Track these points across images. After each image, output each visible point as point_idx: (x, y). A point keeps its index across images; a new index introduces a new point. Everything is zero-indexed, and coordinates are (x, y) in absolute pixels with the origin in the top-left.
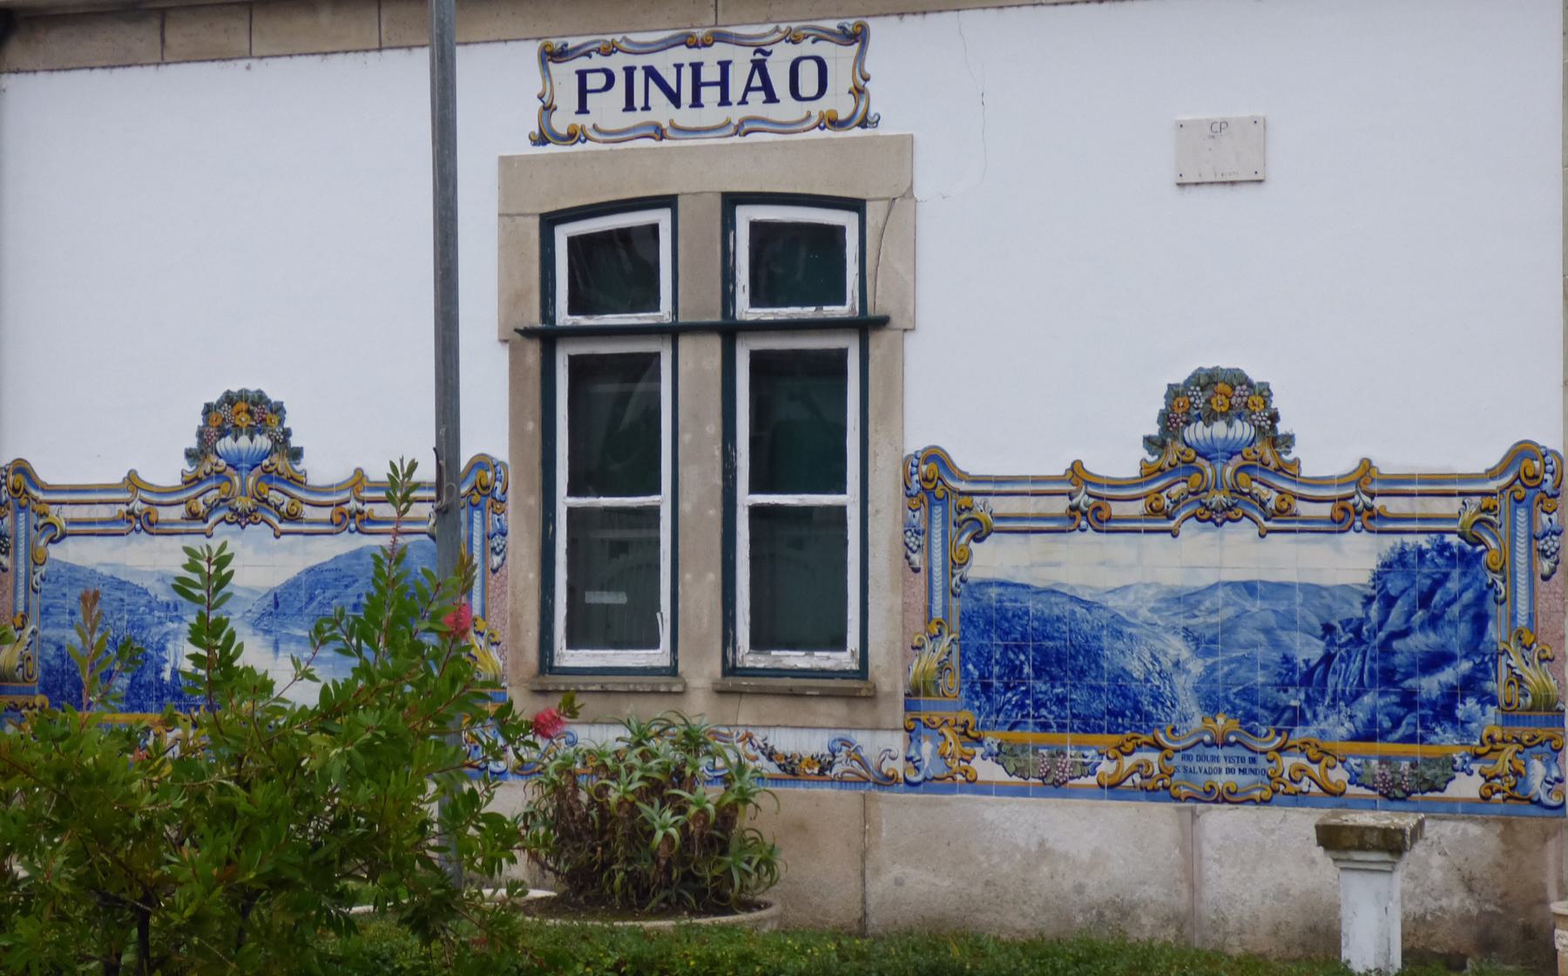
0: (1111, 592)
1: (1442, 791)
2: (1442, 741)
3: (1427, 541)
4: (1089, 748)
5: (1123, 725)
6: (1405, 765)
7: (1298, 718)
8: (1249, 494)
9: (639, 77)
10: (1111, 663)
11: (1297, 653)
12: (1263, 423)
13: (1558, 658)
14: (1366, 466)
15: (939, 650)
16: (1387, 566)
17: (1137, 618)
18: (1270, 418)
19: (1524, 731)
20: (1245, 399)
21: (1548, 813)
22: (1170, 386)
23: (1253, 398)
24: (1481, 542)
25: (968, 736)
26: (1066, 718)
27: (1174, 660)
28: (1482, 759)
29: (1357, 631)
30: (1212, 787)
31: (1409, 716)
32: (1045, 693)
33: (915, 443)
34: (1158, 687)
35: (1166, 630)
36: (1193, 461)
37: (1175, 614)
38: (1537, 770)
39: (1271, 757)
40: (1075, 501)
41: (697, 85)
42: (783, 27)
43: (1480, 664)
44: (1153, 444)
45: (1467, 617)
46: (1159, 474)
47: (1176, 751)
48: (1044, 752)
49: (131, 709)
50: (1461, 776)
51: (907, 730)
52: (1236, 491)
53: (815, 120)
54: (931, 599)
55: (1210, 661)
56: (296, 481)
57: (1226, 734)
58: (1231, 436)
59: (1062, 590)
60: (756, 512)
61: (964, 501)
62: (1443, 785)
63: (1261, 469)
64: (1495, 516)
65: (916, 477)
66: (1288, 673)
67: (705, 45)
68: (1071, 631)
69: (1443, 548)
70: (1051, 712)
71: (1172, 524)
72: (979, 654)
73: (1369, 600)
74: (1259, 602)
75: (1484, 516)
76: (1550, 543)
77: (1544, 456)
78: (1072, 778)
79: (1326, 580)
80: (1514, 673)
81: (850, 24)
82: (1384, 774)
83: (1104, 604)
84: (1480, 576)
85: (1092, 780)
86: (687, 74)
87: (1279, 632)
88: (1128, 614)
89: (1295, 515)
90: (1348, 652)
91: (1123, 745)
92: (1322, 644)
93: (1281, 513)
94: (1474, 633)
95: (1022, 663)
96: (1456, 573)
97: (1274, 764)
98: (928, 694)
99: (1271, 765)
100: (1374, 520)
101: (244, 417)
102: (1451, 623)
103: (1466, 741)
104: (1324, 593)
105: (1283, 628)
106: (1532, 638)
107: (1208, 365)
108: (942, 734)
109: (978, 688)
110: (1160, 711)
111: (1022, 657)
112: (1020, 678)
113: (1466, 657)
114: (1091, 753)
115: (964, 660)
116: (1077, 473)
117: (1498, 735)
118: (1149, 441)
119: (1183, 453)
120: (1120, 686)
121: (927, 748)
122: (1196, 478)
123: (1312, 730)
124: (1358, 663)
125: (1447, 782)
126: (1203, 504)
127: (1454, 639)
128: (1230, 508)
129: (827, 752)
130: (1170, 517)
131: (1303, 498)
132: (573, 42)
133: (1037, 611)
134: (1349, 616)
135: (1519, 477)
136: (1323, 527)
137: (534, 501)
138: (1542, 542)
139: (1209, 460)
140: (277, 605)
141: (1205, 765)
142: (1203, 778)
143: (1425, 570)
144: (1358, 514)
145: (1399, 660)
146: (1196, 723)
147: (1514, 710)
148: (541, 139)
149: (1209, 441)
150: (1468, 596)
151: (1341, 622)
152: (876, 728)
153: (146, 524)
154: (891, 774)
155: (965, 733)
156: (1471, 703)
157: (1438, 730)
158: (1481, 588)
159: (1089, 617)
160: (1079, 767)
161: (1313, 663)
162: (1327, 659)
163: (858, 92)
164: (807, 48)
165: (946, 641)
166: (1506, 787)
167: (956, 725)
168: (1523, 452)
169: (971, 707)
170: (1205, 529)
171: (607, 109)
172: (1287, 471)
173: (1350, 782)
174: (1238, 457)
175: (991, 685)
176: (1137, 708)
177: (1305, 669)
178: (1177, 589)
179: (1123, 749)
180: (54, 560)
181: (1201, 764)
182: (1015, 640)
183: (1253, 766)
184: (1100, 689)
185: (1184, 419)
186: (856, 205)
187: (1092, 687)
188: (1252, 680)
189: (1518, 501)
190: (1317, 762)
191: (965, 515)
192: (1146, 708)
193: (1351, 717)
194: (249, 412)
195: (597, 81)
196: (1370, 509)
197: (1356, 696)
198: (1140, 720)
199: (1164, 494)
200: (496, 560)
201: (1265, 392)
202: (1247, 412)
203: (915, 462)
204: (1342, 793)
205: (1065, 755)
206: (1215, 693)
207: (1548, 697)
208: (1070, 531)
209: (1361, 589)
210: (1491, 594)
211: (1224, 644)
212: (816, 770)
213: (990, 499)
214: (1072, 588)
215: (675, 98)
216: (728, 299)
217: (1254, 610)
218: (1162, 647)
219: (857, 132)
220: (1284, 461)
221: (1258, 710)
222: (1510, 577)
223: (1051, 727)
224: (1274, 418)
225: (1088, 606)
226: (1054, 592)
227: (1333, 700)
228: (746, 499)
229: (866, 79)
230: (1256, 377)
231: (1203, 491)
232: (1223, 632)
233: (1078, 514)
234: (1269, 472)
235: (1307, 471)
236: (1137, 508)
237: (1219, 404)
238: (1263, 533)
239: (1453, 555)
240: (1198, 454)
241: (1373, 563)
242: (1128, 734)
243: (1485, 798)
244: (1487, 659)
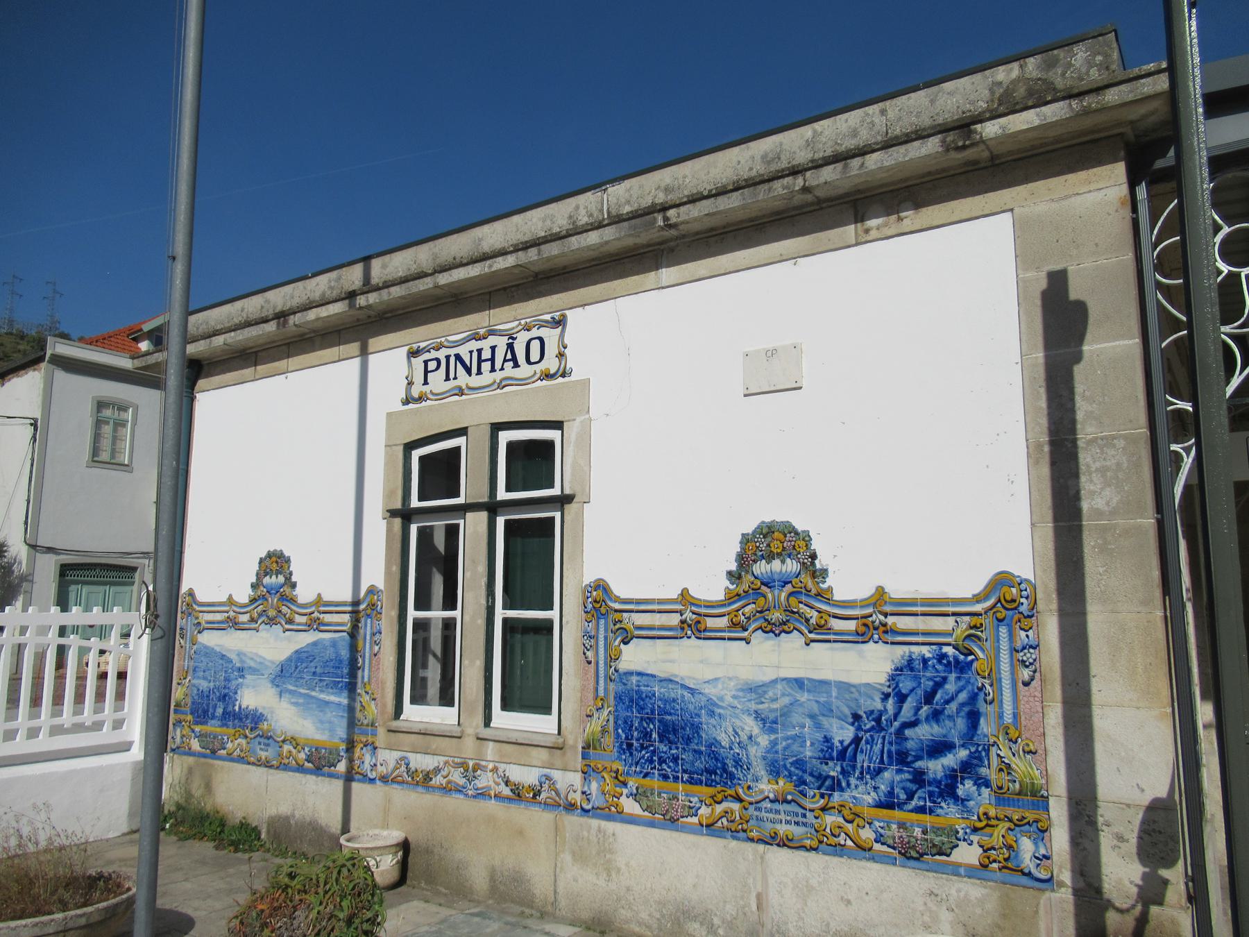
0: (708, 682)
1: (948, 855)
2: (947, 814)
3: (929, 652)
4: (693, 796)
5: (715, 781)
6: (917, 832)
7: (836, 786)
8: (797, 613)
9: (452, 360)
10: (707, 734)
11: (834, 735)
12: (806, 561)
13: (1040, 752)
14: (881, 591)
15: (602, 719)
16: (899, 669)
17: (723, 702)
18: (810, 557)
19: (1014, 812)
20: (793, 543)
21: (1037, 884)
22: (743, 535)
23: (798, 542)
24: (971, 653)
25: (618, 780)
26: (677, 772)
27: (749, 734)
28: (979, 832)
29: (878, 720)
30: (775, 833)
31: (920, 791)
32: (665, 753)
33: (589, 578)
34: (738, 754)
35: (743, 712)
36: (759, 589)
37: (750, 700)
38: (1027, 847)
39: (817, 815)
40: (684, 617)
41: (480, 361)
42: (523, 322)
43: (975, 752)
44: (733, 576)
45: (962, 714)
46: (737, 597)
47: (751, 803)
48: (665, 795)
49: (222, 726)
50: (962, 844)
51: (583, 772)
52: (788, 610)
53: (538, 376)
54: (597, 682)
55: (773, 737)
56: (293, 600)
57: (785, 794)
58: (784, 570)
59: (676, 680)
61: (617, 616)
62: (949, 850)
63: (805, 594)
64: (982, 632)
65: (590, 600)
66: (828, 751)
67: (485, 338)
68: (681, 709)
69: (941, 657)
70: (669, 767)
71: (745, 634)
72: (625, 722)
73: (886, 696)
74: (806, 694)
75: (972, 631)
76: (1028, 655)
77: (1019, 584)
78: (682, 817)
79: (855, 679)
80: (1003, 762)
81: (557, 315)
82: (901, 837)
83: (703, 691)
84: (972, 681)
85: (695, 820)
86: (475, 355)
87: (820, 718)
88: (718, 699)
89: (830, 629)
90: (871, 736)
91: (715, 796)
92: (852, 729)
93: (820, 627)
94: (968, 727)
95: (651, 730)
96: (952, 677)
97: (819, 820)
98: (595, 748)
99: (817, 821)
100: (887, 634)
101: (275, 565)
102: (950, 717)
103: (965, 816)
104: (853, 690)
105: (824, 715)
106: (1017, 735)
107: (768, 519)
108: (603, 777)
109: (625, 747)
110: (739, 772)
111: (652, 726)
112: (650, 741)
113: (963, 746)
114: (695, 800)
115: (616, 727)
116: (685, 597)
117: (992, 813)
118: (730, 574)
119: (752, 583)
120: (713, 751)
121: (594, 785)
122: (761, 601)
123: (846, 795)
124: (879, 746)
125: (952, 849)
126: (766, 620)
127: (953, 731)
128: (784, 623)
129: (538, 783)
130: (746, 630)
131: (835, 617)
132: (423, 345)
133: (661, 693)
134: (872, 708)
135: (999, 601)
136: (850, 638)
137: (394, 613)
138: (1022, 654)
139: (770, 587)
140: (282, 671)
141: (771, 816)
142: (769, 825)
143: (928, 674)
144: (876, 629)
145: (910, 745)
147: (1004, 793)
148: (406, 402)
149: (769, 574)
150: (963, 696)
151: (865, 712)
152: (565, 769)
153: (234, 624)
154: (573, 802)
155: (616, 778)
156: (969, 784)
157: (943, 804)
158: (973, 690)
159: (693, 700)
160: (687, 809)
161: (846, 743)
162: (857, 740)
163: (561, 355)
164: (535, 332)
165: (606, 712)
166: (1001, 858)
167: (611, 771)
168: (1002, 580)
169: (621, 760)
170: (767, 639)
173: (876, 841)
174: (790, 585)
175: (632, 744)
176: (725, 770)
177: (840, 748)
178: (749, 682)
179: (715, 798)
180: (201, 643)
181: (767, 815)
182: (647, 714)
183: (804, 820)
184: (700, 752)
185: (753, 558)
186: (558, 425)
187: (695, 751)
188: (802, 753)
189: (1000, 621)
190: (851, 822)
191: (618, 626)
192: (730, 769)
193: (875, 788)
194: (277, 562)
195: (432, 365)
196: (885, 625)
197: (879, 771)
198: (726, 778)
199: (740, 612)
200: (376, 648)
201: (807, 539)
202: (795, 552)
203: (590, 589)
204: (870, 849)
205: (678, 800)
206: (776, 761)
207: (1033, 784)
208: (681, 638)
209: (880, 687)
210: (981, 695)
211: (783, 725)
212: (531, 795)
213: (633, 614)
214: (682, 679)
215: (469, 371)
217: (803, 699)
218: (741, 724)
219: (560, 380)
220: (822, 589)
221: (808, 779)
222: (996, 682)
223: (669, 778)
224: (814, 556)
225: (692, 691)
226: (671, 681)
227: (862, 773)
228: (500, 614)
229: (565, 348)
231: (766, 610)
232: (781, 716)
233: (685, 626)
234: (811, 596)
235: (838, 596)
236: (723, 622)
237: (776, 547)
238: (808, 642)
239: (949, 663)
240: (762, 583)
241: (888, 668)
242: (719, 788)
243: (984, 866)
244: (980, 749)
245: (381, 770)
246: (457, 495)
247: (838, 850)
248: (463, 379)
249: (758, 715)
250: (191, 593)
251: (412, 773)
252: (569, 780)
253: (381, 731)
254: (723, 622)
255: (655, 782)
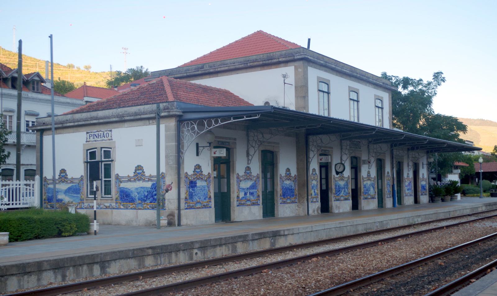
7: (146, 201)
33: (116, 173)
56: (67, 178)
60: (105, 181)
93: (144, 180)
121: (117, 205)
132: (89, 132)
146: (138, 202)
148: (87, 142)
163: (111, 137)
171: (92, 138)
172: (144, 175)
195: (91, 136)
201: (142, 167)
215: (97, 137)
216: (101, 158)
230: (142, 166)
235: (146, 175)
236: (133, 180)
241: (151, 185)
245: (85, 207)
246: (95, 159)
247: (146, 209)
248: (96, 139)
249: (137, 193)
250: (45, 177)
251: (90, 206)
252: (114, 205)
253: (85, 200)
254: (133, 180)
255: (125, 203)
